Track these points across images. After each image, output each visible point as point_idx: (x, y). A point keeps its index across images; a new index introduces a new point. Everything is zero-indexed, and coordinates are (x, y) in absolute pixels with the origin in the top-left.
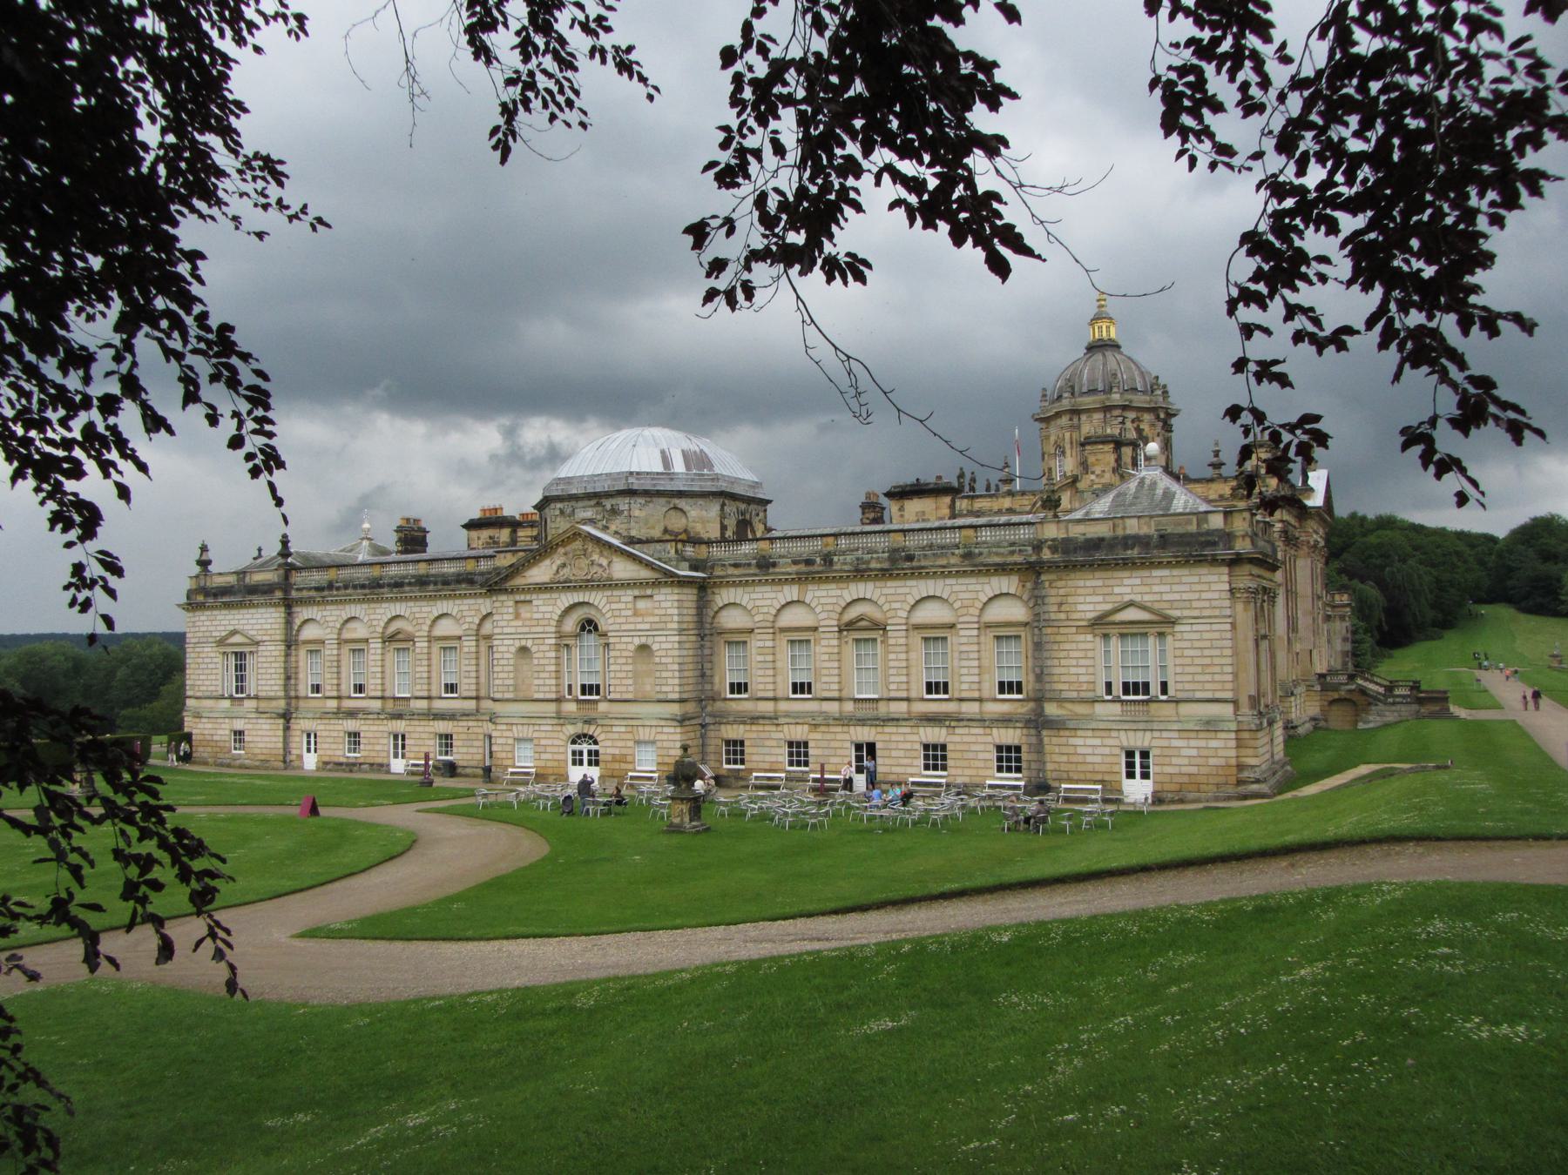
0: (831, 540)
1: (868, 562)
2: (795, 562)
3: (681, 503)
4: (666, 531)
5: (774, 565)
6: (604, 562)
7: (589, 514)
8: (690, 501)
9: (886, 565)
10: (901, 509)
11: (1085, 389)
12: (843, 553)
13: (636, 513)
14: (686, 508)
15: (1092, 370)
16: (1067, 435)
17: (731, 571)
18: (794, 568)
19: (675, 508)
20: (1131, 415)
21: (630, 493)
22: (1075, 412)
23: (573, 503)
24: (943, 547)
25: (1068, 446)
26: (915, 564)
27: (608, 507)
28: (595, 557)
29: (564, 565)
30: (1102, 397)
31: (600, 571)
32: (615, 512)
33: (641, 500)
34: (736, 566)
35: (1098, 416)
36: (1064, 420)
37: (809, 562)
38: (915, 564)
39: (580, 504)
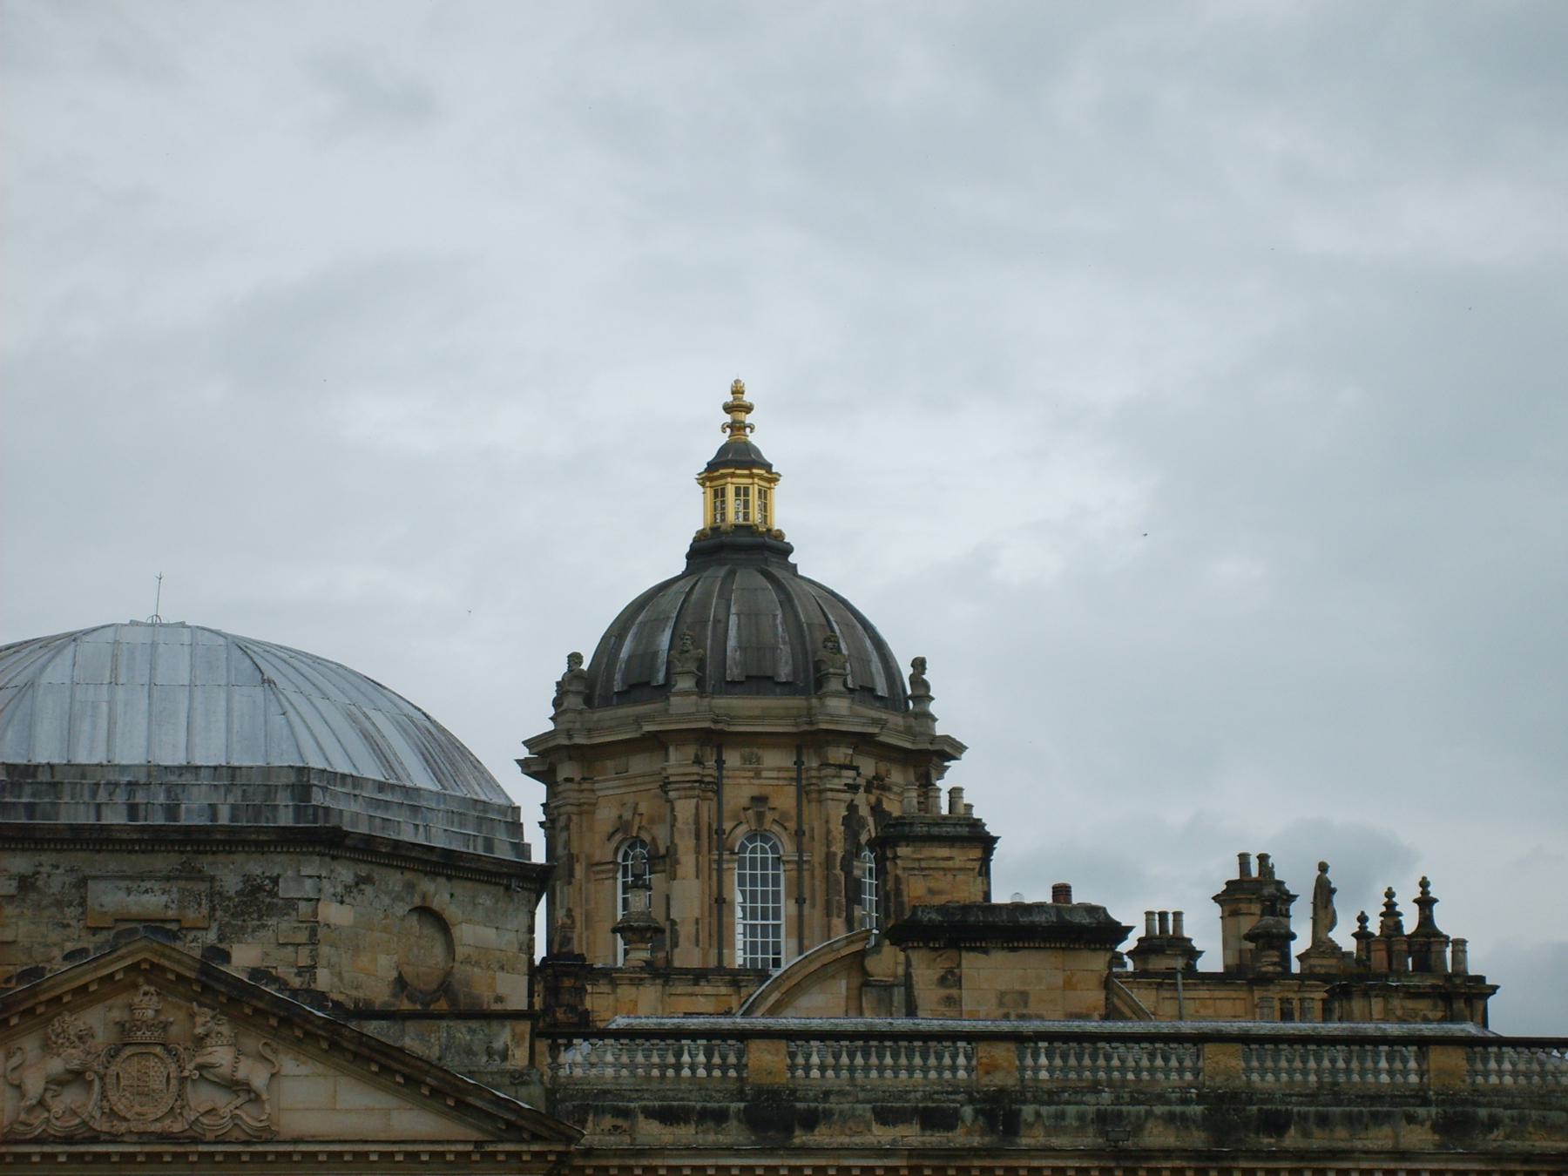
0: (1003, 1053)
1: (1138, 1129)
2: (886, 1116)
3: (439, 893)
4: (401, 983)
5: (810, 1121)
6: (258, 1077)
7: (152, 901)
8: (462, 889)
9: (1197, 1139)
10: (950, 979)
11: (733, 673)
12: (1051, 1097)
13: (335, 914)
14: (452, 912)
15: (751, 617)
16: (685, 809)
17: (651, 1131)
18: (882, 1135)
19: (426, 912)
20: (868, 767)
21: (323, 839)
22: (714, 739)
23: (82, 860)
24: (1376, 1098)
25: (685, 845)
26: (1293, 1139)
27: (231, 882)
28: (221, 1056)
29: (76, 1077)
30: (796, 702)
31: (223, 1101)
32: (258, 901)
33: (345, 873)
34: (668, 1116)
35: (776, 760)
36: (678, 761)
37: (933, 1118)
38: (1293, 1139)
39: (112, 863)
